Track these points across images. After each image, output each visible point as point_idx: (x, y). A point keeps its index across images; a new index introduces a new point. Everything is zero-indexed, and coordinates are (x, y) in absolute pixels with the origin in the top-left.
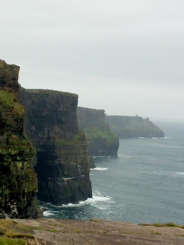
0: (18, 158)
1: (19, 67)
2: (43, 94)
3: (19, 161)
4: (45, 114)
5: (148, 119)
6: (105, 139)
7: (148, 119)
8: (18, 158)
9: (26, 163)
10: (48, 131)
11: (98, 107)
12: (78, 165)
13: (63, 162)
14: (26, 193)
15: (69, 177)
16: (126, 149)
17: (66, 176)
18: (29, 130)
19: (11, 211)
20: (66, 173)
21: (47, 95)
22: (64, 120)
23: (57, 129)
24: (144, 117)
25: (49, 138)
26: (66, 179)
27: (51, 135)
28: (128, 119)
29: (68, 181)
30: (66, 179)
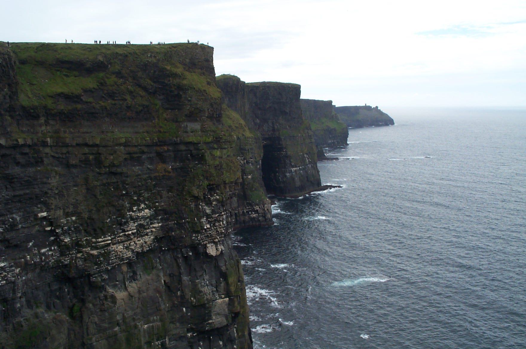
0: (215, 146)
1: (212, 48)
2: (265, 86)
3: (217, 149)
4: (268, 106)
5: (377, 107)
6: (335, 129)
7: (377, 107)
8: (215, 146)
9: (225, 151)
10: (273, 123)
13: (289, 153)
14: (228, 184)
16: (355, 137)
17: (293, 167)
18: (253, 123)
19: (212, 204)
20: (293, 164)
22: (288, 111)
24: (373, 106)
25: (274, 130)
27: (276, 127)
28: (357, 109)
30: (293, 169)
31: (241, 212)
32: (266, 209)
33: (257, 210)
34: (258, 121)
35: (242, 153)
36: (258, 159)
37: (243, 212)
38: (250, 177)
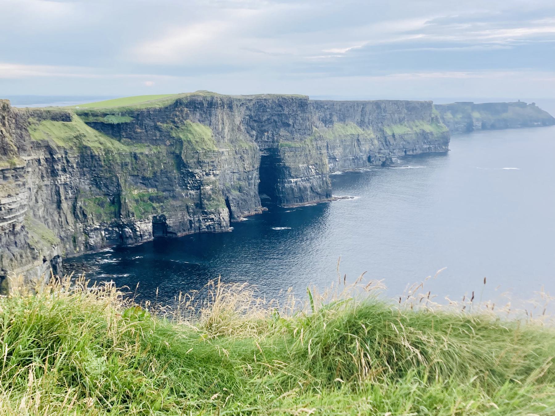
5: (534, 104)
6: (431, 133)
7: (534, 104)
11: (427, 100)
12: (310, 167)
13: (287, 164)
15: (297, 178)
20: (292, 175)
21: (265, 100)
22: (291, 123)
23: (283, 132)
25: (273, 142)
26: (295, 180)
27: (276, 138)
28: (505, 106)
29: (296, 182)
31: (197, 219)
32: (221, 218)
33: (213, 219)
34: (254, 133)
35: (201, 166)
36: (247, 169)
37: (199, 220)
38: (208, 188)
